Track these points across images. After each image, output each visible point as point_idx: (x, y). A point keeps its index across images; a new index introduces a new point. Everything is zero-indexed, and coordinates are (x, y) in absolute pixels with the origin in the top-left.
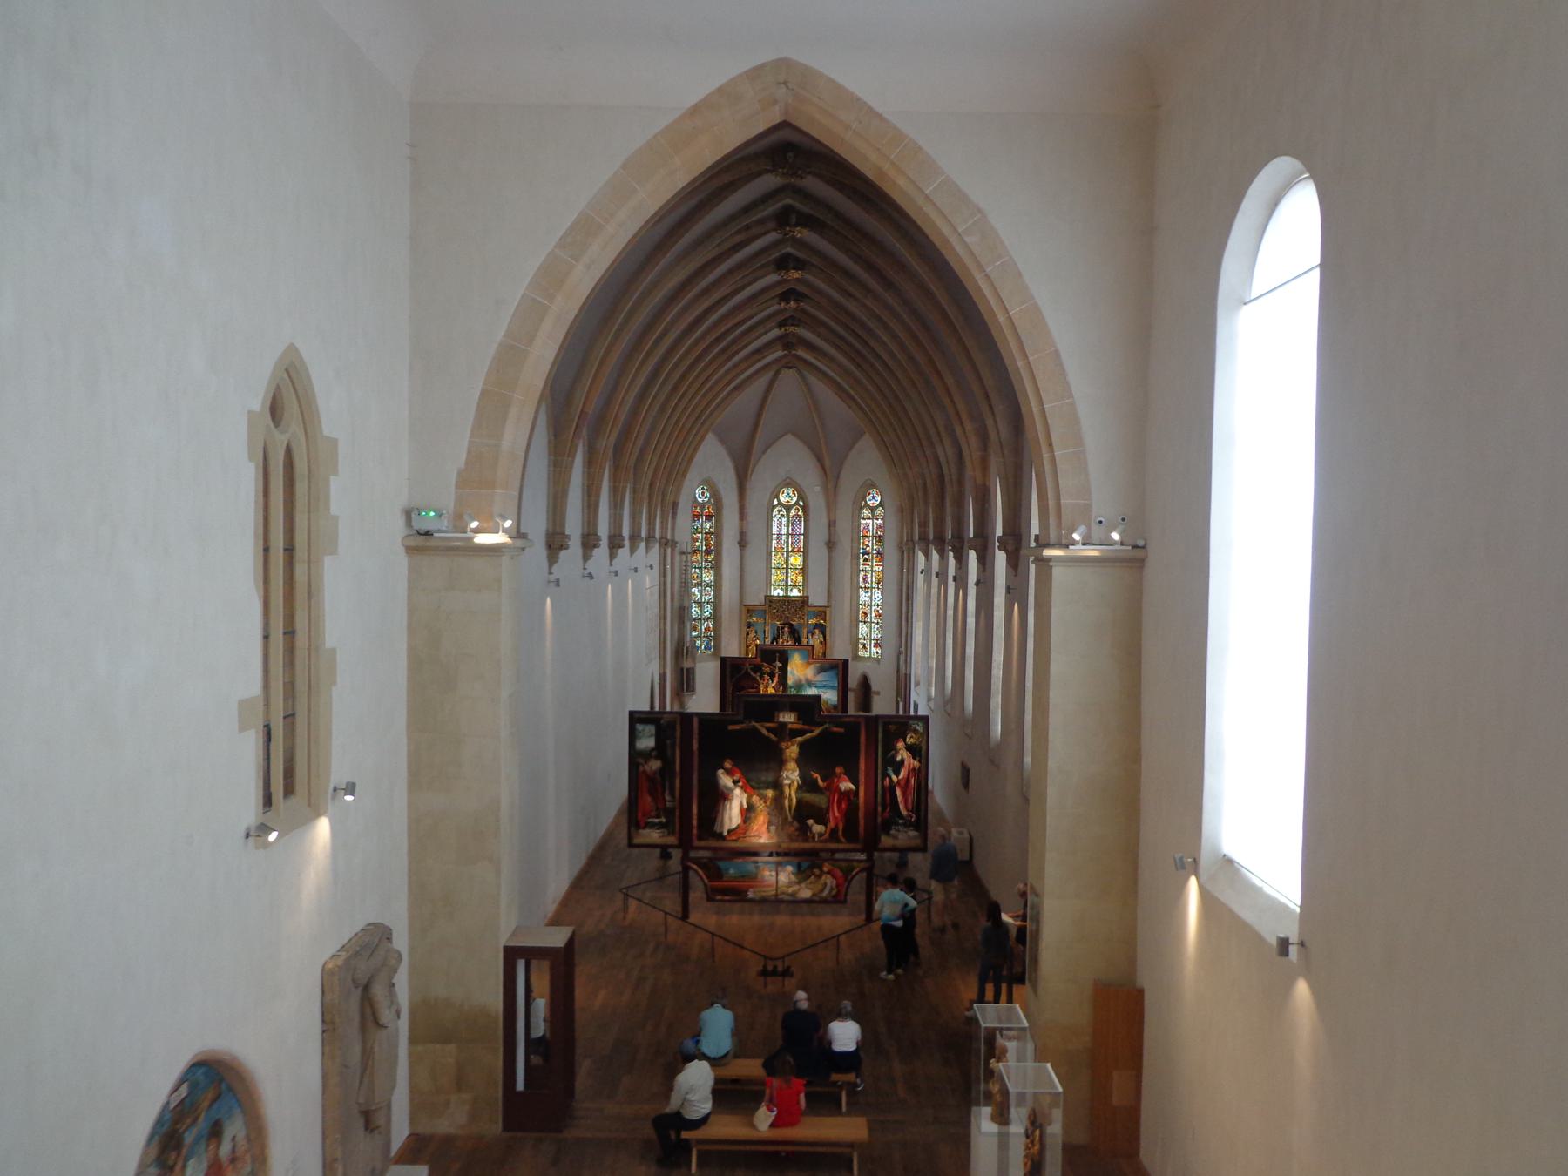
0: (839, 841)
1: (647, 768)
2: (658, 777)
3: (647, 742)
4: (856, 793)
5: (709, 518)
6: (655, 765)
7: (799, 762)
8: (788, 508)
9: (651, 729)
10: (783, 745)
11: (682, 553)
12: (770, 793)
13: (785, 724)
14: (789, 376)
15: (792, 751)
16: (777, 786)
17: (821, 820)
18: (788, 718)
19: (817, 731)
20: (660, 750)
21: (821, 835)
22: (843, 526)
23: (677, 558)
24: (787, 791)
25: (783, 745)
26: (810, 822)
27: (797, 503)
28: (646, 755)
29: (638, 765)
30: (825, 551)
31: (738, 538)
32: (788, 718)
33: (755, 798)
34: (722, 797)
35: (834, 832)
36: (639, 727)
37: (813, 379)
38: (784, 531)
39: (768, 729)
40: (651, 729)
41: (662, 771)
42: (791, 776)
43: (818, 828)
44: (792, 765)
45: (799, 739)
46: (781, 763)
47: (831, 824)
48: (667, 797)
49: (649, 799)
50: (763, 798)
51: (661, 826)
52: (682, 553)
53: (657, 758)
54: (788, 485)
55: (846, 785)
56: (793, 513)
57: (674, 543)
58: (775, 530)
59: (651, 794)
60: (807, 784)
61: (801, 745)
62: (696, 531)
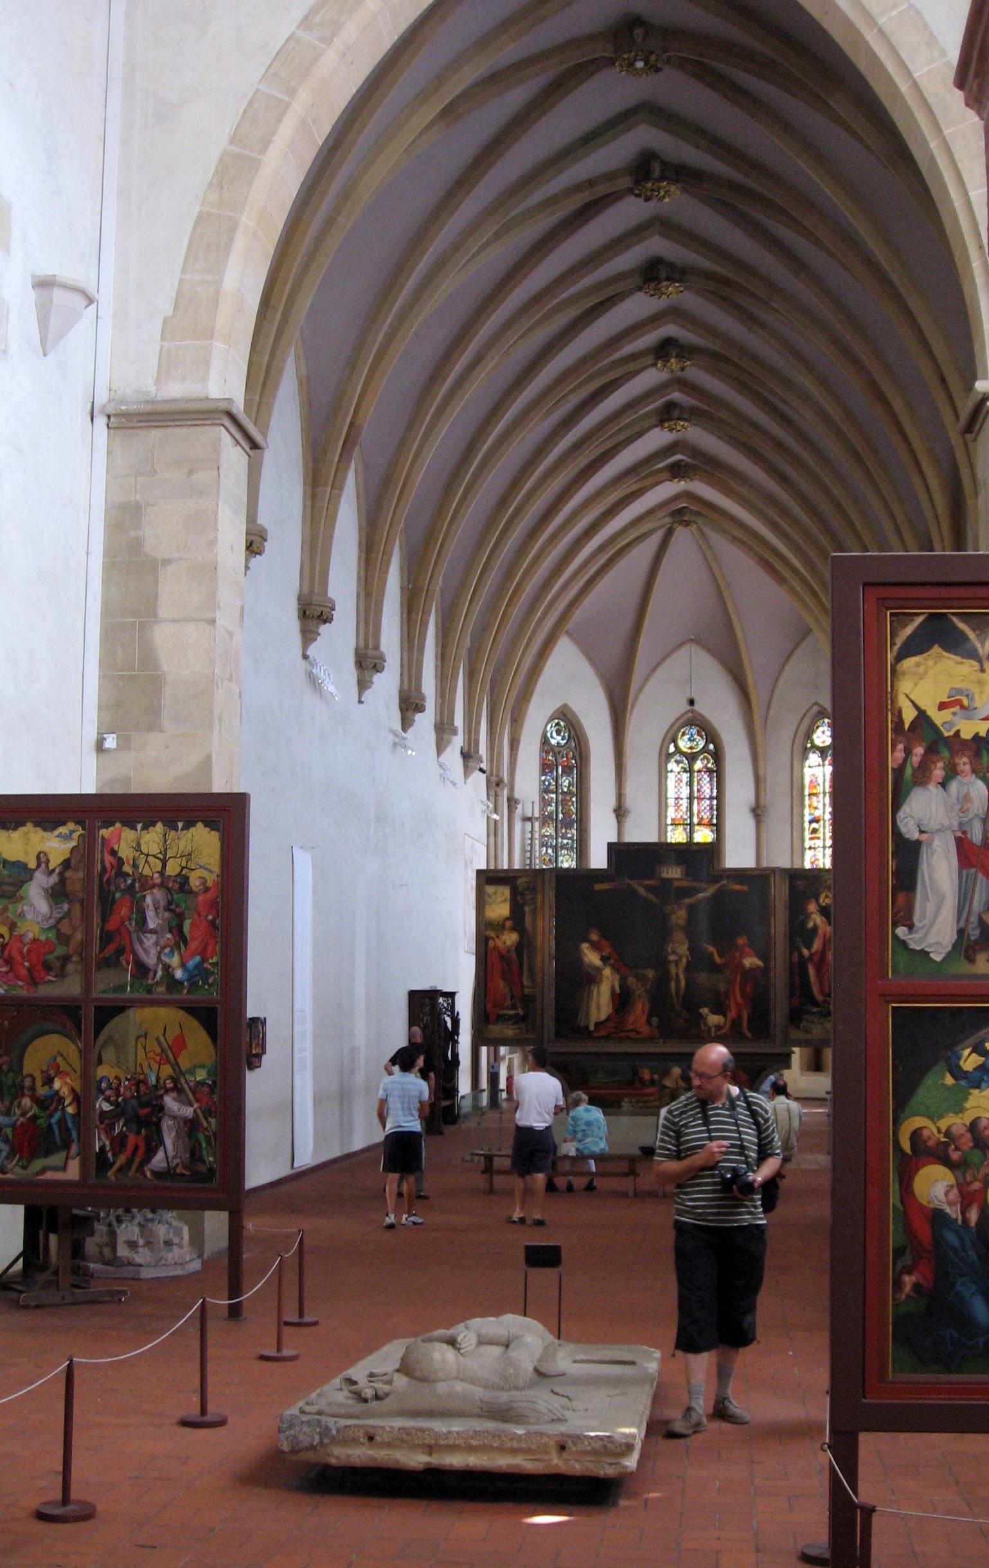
0: (743, 1037)
1: (500, 944)
2: (514, 956)
3: (500, 909)
4: (765, 971)
5: (567, 771)
6: (510, 938)
7: (690, 930)
8: (692, 758)
9: (505, 891)
10: (668, 909)
11: (526, 819)
12: (650, 973)
13: (669, 881)
14: (682, 535)
15: (680, 916)
16: (661, 964)
17: (719, 1009)
18: (673, 872)
19: (712, 890)
20: (517, 918)
21: (718, 1027)
22: (777, 782)
23: (518, 825)
24: (673, 969)
25: (668, 909)
26: (705, 1011)
27: (705, 750)
28: (498, 927)
29: (487, 939)
30: (750, 823)
31: (612, 802)
32: (673, 872)
33: (631, 980)
34: (591, 978)
35: (736, 1023)
36: (490, 889)
37: (715, 537)
38: (685, 792)
39: (647, 888)
40: (505, 891)
41: (519, 947)
42: (679, 949)
43: (714, 1019)
44: (679, 936)
45: (688, 901)
46: (666, 932)
47: (732, 1014)
48: (526, 982)
49: (502, 982)
50: (641, 978)
51: (518, 1020)
52: (526, 819)
53: (513, 929)
54: (691, 723)
55: (750, 961)
56: (698, 765)
57: (512, 802)
58: (671, 793)
59: (503, 979)
60: (697, 962)
61: (691, 909)
62: (547, 791)
